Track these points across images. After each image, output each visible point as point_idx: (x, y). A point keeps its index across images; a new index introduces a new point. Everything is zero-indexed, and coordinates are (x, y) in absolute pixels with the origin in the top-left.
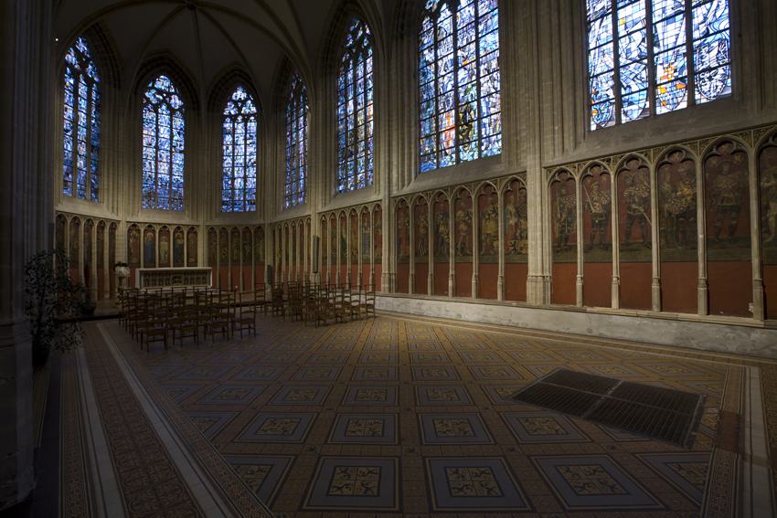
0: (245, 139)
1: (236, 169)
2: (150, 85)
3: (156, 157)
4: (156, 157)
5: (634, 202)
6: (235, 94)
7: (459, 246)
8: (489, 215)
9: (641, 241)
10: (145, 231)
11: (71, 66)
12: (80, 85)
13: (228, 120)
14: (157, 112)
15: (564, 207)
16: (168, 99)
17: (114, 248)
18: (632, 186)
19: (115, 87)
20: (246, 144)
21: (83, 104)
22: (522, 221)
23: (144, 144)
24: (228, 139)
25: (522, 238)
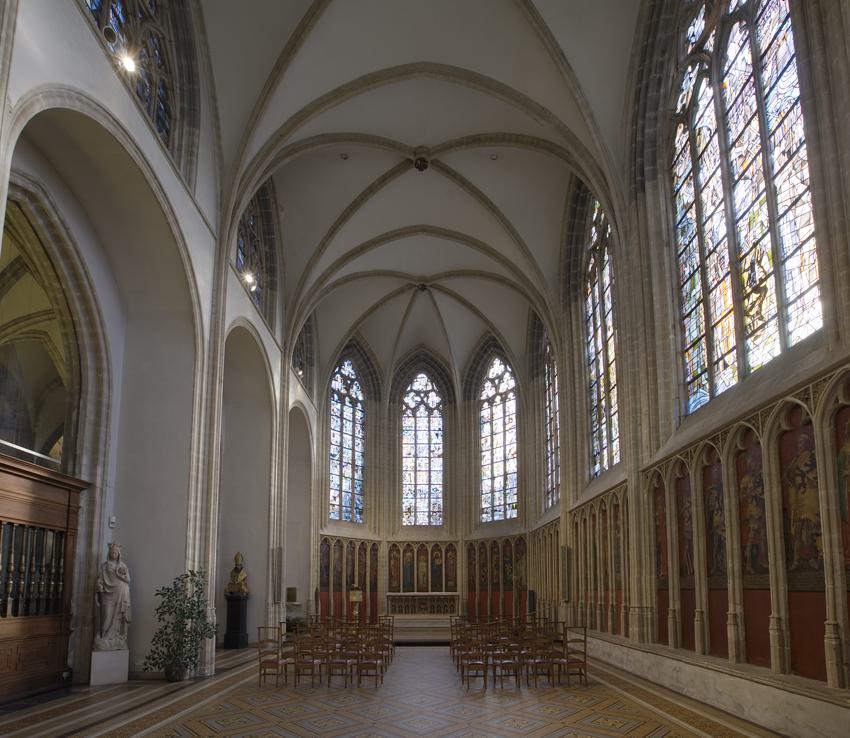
0: (505, 424)
1: (495, 465)
2: (409, 389)
3: (415, 467)
4: (415, 467)
6: (492, 370)
8: (803, 475)
10: (404, 551)
11: (338, 392)
12: (345, 408)
13: (486, 405)
14: (415, 416)
16: (425, 399)
17: (376, 571)
19: (376, 400)
20: (505, 431)
21: (348, 426)
23: (404, 455)
24: (486, 429)
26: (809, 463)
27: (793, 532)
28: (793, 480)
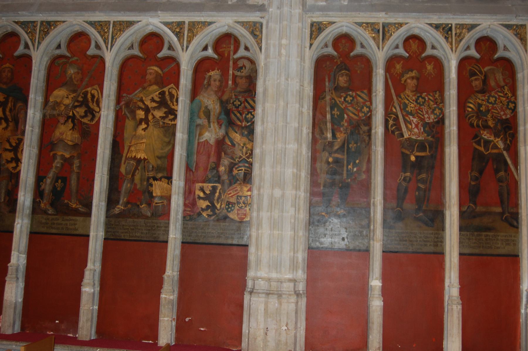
5: (486, 127)
7: (47, 185)
8: (147, 110)
9: (499, 210)
15: (341, 117)
18: (483, 91)
22: (237, 137)
25: (233, 180)
26: (157, 99)
27: (123, 170)
28: (133, 113)
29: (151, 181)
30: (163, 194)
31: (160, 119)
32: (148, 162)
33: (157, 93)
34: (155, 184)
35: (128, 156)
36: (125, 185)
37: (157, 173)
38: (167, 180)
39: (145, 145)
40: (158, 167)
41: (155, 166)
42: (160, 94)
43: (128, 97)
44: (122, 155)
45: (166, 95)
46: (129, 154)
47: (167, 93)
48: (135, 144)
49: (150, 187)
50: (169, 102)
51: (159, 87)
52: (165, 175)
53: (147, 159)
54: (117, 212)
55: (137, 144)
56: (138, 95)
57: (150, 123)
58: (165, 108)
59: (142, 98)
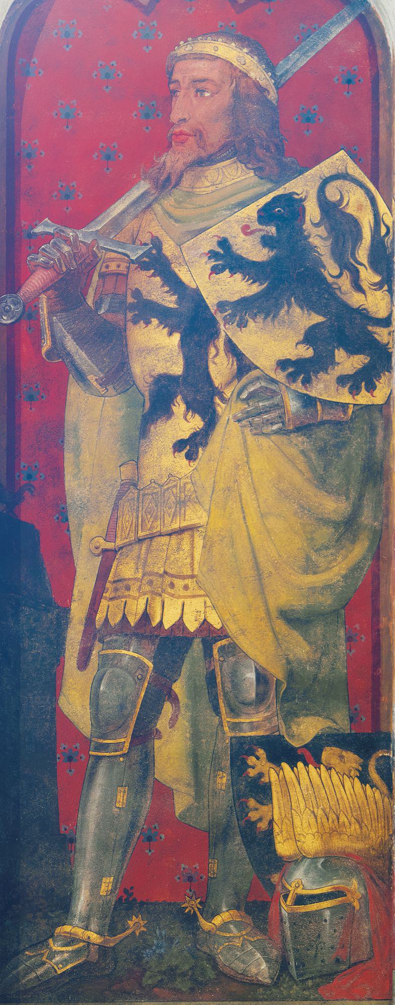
29: (259, 764)
30: (339, 843)
31: (281, 376)
32: (232, 649)
33: (252, 211)
34: (284, 782)
35: (100, 617)
36: (97, 794)
37: (290, 716)
38: (352, 760)
39: (199, 542)
40: (291, 675)
41: (277, 672)
42: (265, 215)
43: (67, 241)
44: (65, 612)
45: (307, 226)
46: (104, 603)
47: (312, 211)
48: (140, 541)
49: (252, 803)
50: (331, 269)
51: (258, 171)
52: (341, 722)
53: (222, 634)
54: (65, 962)
55: (151, 538)
56: (130, 225)
57: (220, 407)
58: (309, 305)
59: (157, 243)
